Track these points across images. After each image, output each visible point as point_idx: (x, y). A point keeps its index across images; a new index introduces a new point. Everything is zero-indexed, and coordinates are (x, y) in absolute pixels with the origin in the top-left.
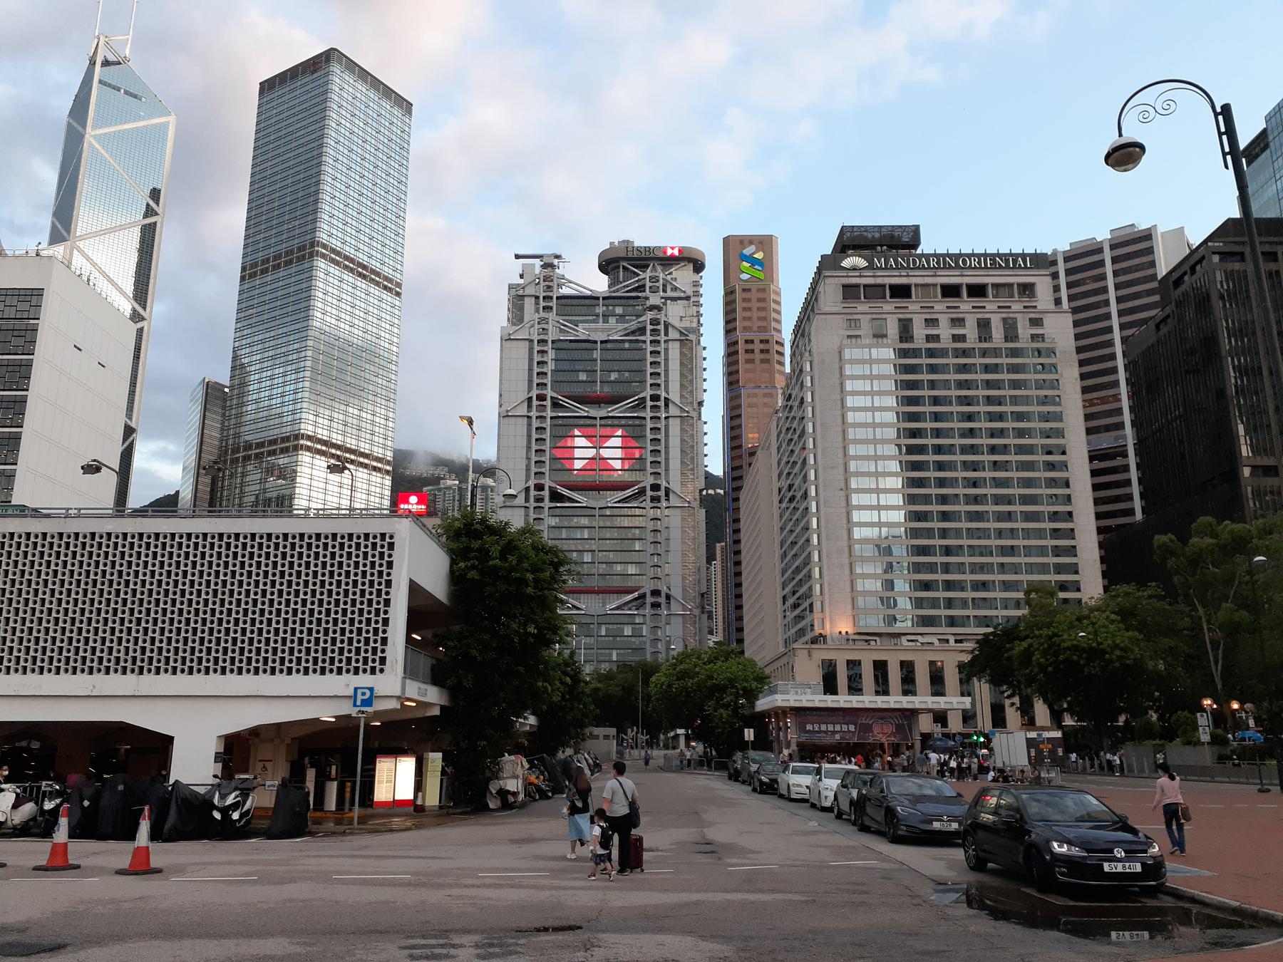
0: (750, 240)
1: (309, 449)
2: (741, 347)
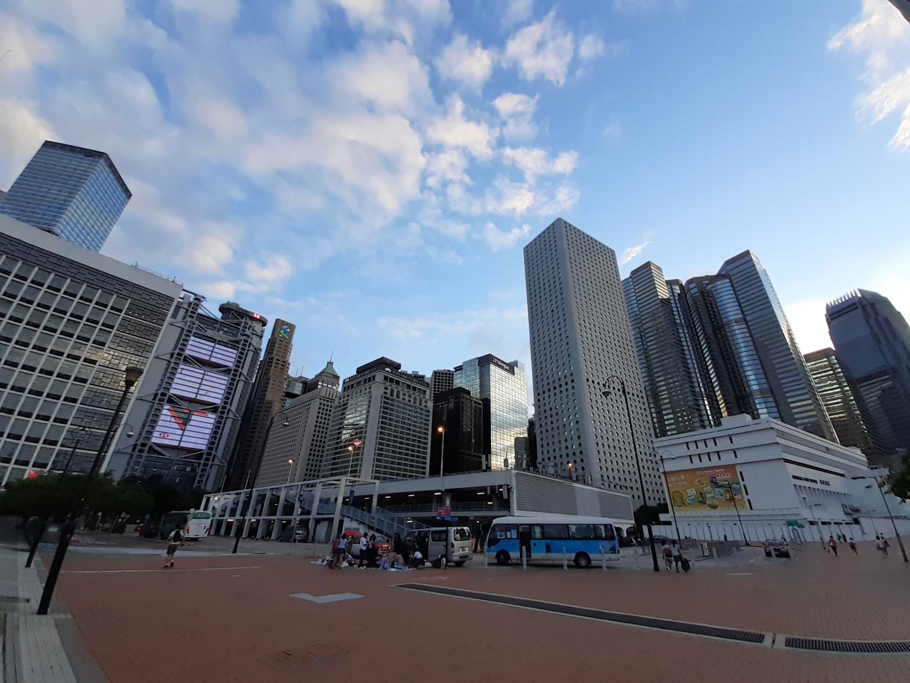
0: (287, 324)
2: (274, 361)
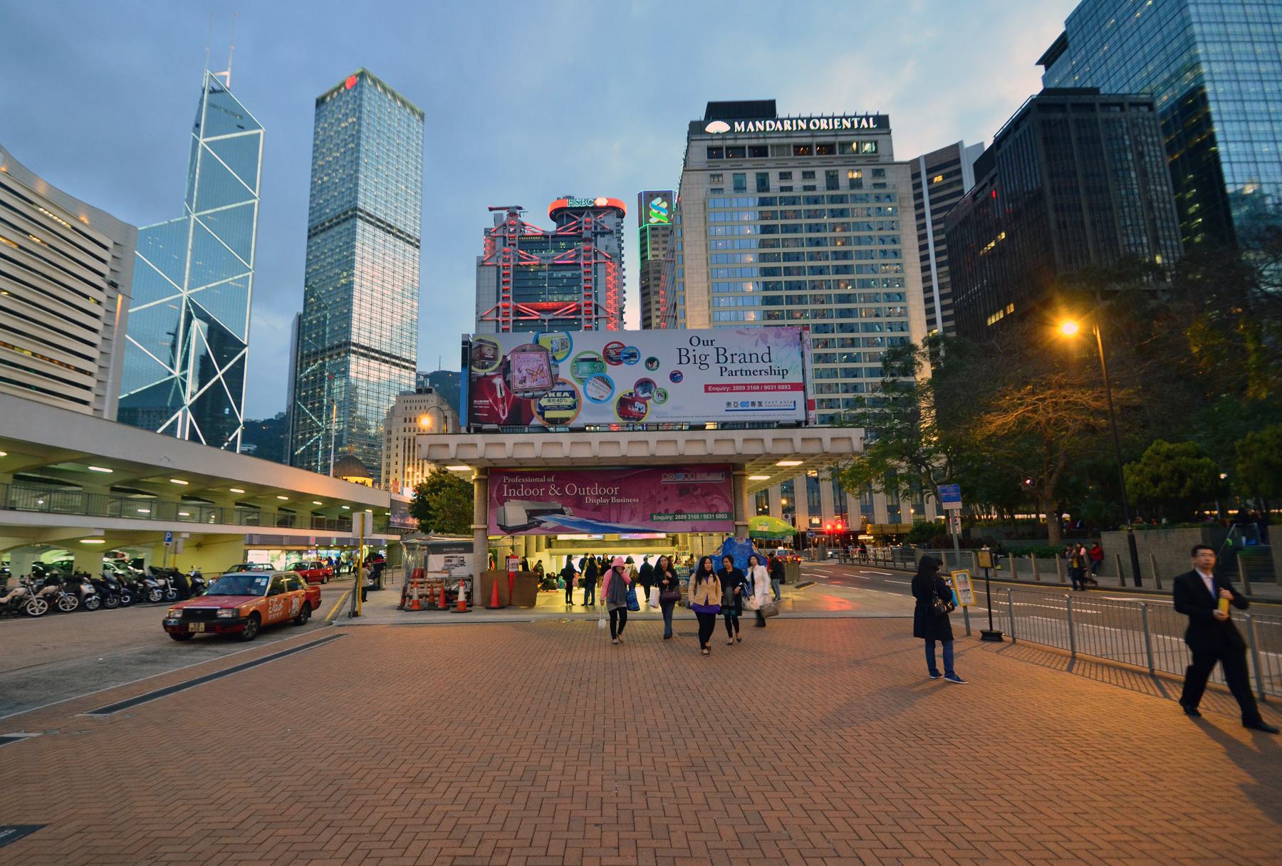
1: (354, 352)
